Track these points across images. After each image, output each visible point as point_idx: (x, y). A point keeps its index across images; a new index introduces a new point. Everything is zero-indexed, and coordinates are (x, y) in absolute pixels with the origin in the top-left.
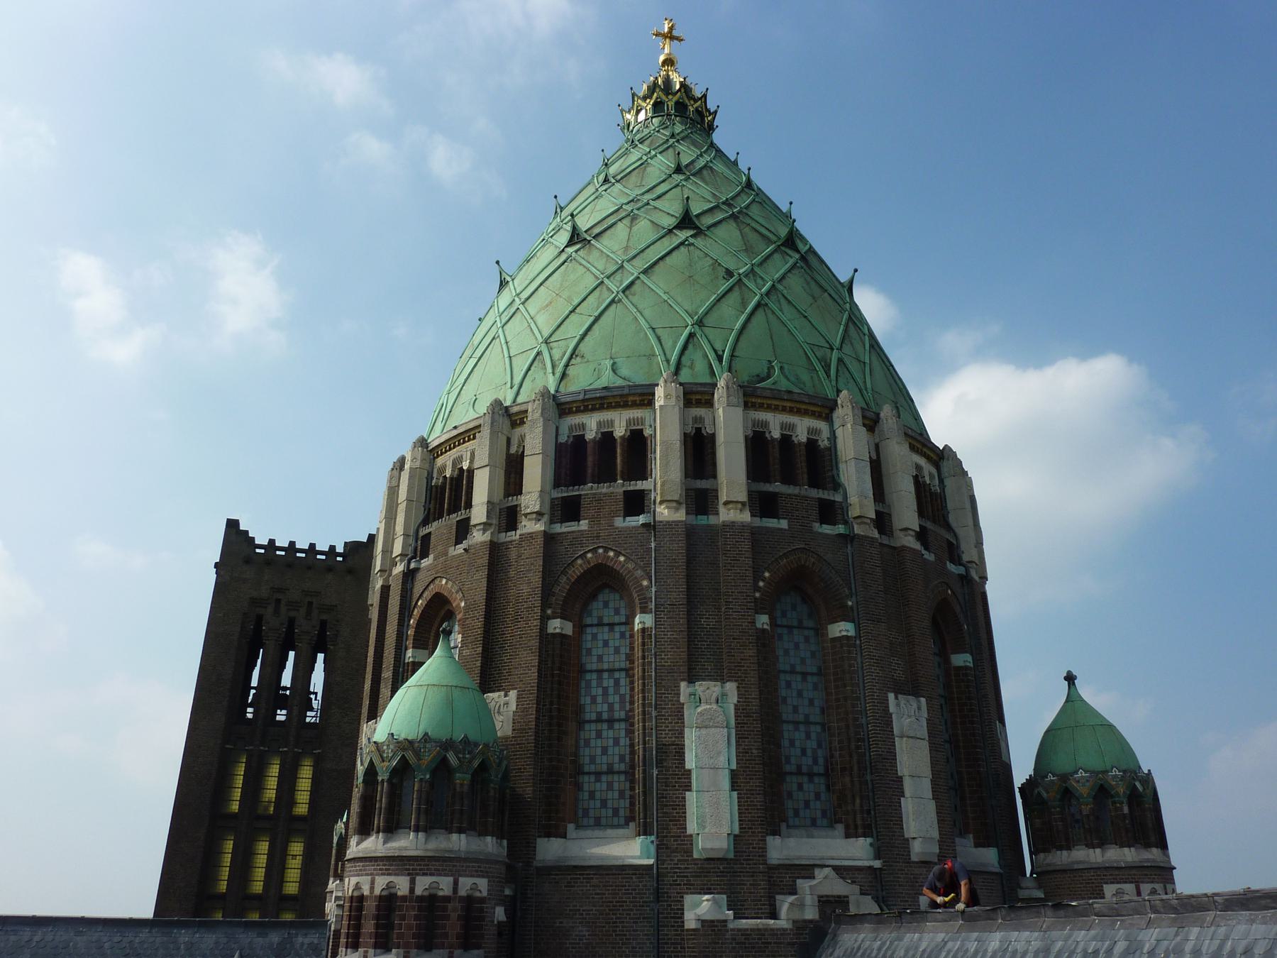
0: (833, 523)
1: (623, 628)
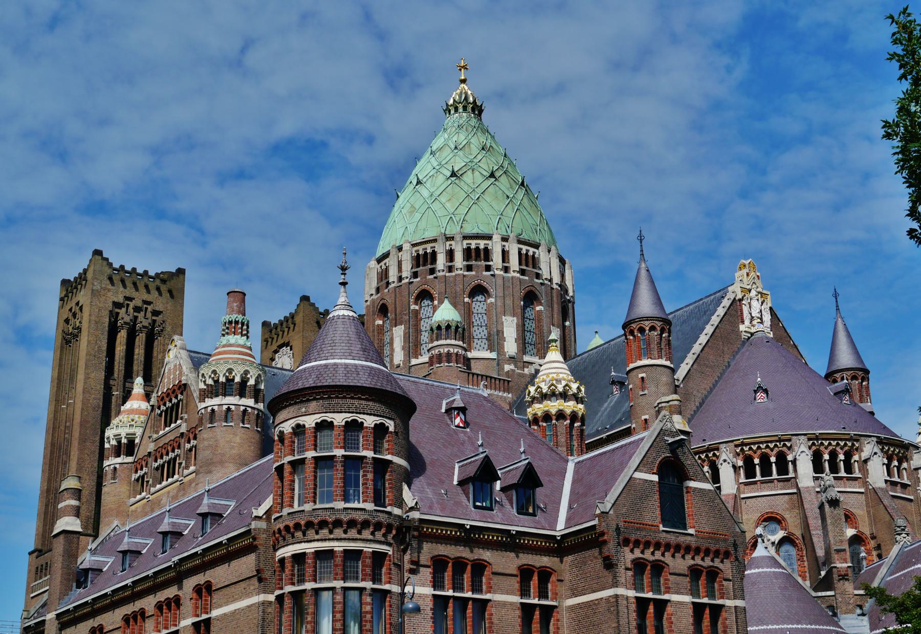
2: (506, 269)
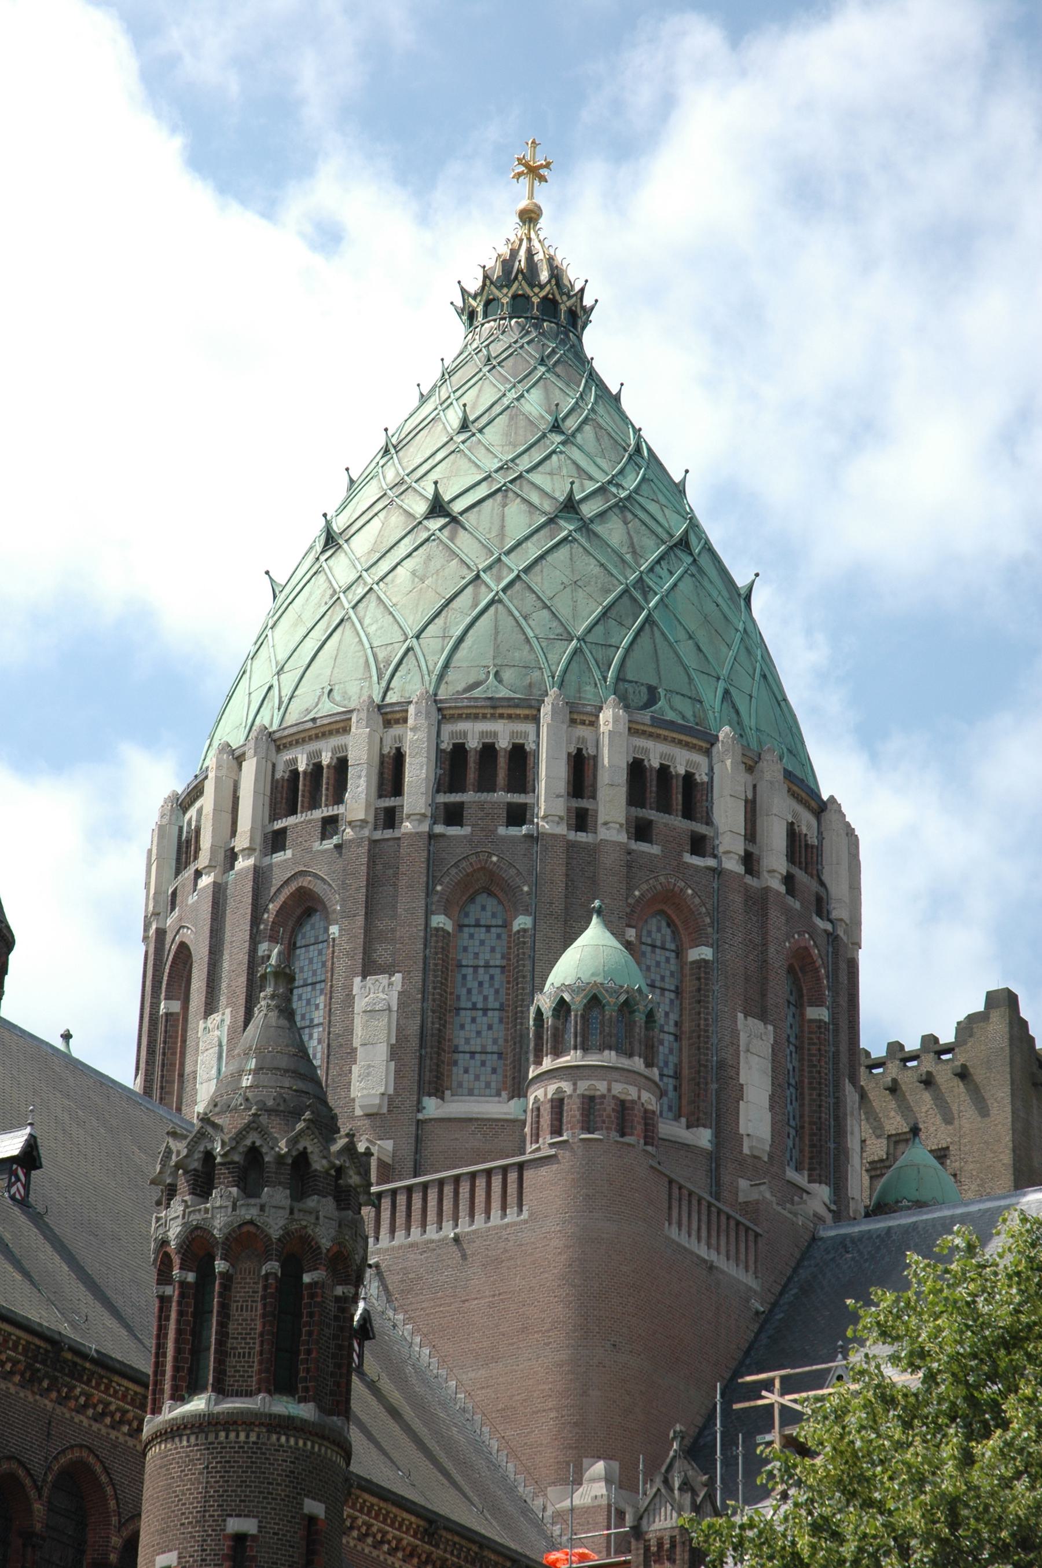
0: (703, 855)
1: (499, 930)
2: (581, 820)
